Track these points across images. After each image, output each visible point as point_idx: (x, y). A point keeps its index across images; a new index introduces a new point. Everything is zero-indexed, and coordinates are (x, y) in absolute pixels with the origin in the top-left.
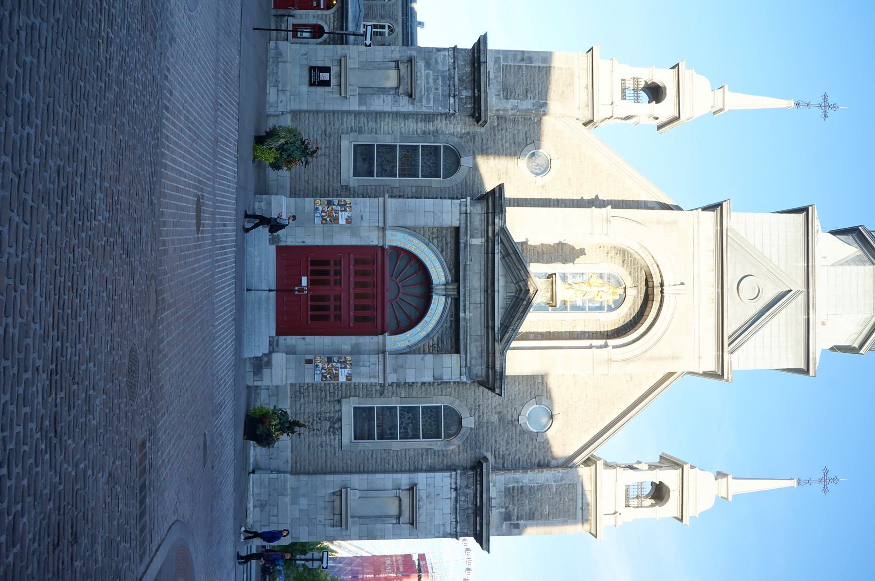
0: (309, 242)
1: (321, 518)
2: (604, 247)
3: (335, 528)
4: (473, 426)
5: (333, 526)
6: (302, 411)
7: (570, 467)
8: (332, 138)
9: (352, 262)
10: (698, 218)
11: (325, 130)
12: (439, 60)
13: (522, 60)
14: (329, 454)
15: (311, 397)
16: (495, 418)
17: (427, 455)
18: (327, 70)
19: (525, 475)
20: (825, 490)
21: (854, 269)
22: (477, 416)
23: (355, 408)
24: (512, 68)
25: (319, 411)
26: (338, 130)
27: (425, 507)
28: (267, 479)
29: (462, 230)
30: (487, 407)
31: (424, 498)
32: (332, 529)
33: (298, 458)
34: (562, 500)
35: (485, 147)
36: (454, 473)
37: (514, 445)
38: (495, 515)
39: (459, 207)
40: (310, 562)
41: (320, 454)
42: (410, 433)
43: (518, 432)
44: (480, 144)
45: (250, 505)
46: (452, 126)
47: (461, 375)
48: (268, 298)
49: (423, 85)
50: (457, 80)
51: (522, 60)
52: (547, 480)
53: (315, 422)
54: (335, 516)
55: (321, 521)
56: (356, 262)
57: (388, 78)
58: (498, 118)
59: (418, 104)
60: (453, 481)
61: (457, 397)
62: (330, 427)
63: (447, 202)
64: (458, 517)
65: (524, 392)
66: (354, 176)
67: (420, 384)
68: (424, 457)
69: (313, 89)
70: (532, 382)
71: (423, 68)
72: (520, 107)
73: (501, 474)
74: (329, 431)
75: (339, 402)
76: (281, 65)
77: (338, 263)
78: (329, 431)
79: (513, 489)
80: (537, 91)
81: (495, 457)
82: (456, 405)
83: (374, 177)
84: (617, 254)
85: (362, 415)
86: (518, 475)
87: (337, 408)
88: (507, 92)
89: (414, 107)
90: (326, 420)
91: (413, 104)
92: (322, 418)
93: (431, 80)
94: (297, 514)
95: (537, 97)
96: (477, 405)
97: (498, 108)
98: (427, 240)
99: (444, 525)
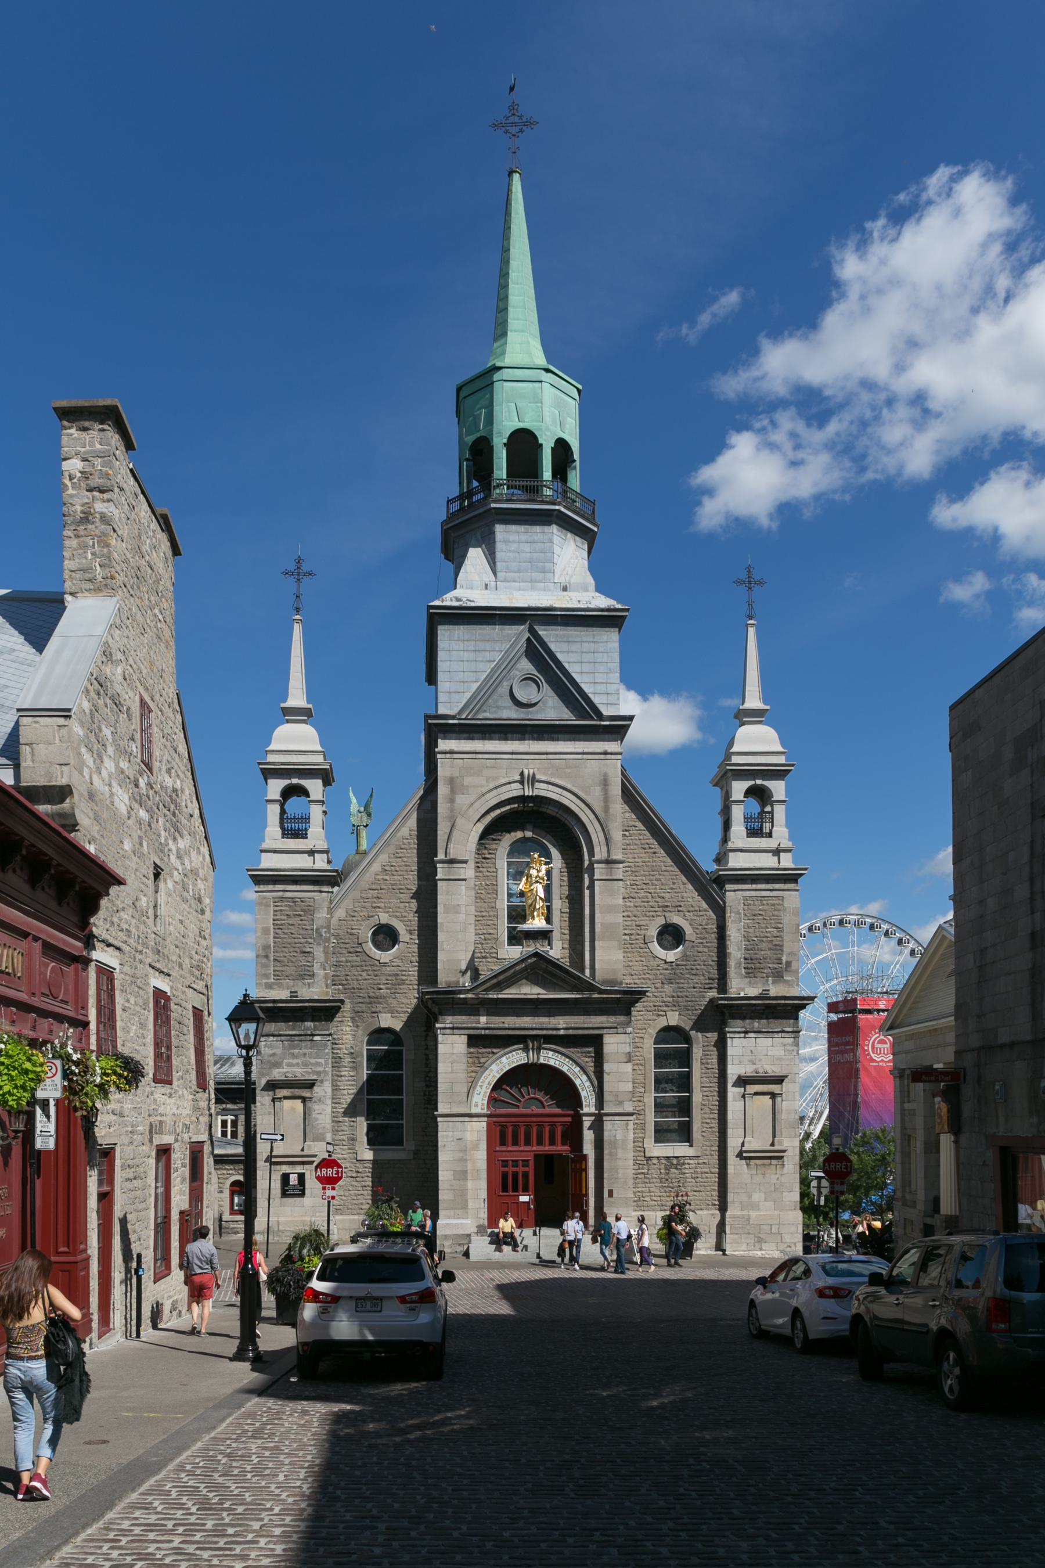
0: (484, 1194)
1: (774, 1178)
2: (478, 863)
4: (677, 1013)
6: (659, 1198)
7: (724, 902)
8: (360, 1170)
9: (504, 1148)
10: (446, 753)
11: (352, 1177)
12: (271, 1052)
13: (267, 957)
14: (704, 1170)
15: (644, 1189)
16: (668, 989)
17: (708, 1064)
18: (285, 1178)
20: (760, 583)
21: (499, 546)
22: (665, 1009)
23: (656, 1141)
24: (276, 968)
25: (659, 1181)
26: (352, 1163)
27: (765, 1066)
28: (732, 1236)
30: (656, 997)
31: (755, 1067)
32: (786, 1166)
33: (710, 1203)
34: (761, 913)
35: (367, 1000)
36: (728, 1035)
37: (698, 967)
38: (775, 990)
40: (822, 1190)
41: (706, 1180)
42: (685, 1083)
43: (684, 963)
44: (364, 1005)
45: (759, 1253)
46: (345, 1037)
48: (546, 1237)
49: (300, 1070)
50: (294, 1033)
51: (267, 957)
53: (671, 1185)
56: (503, 1143)
57: (293, 1109)
58: (334, 985)
59: (323, 1075)
60: (737, 1035)
61: (644, 1031)
62: (676, 1168)
63: (442, 1049)
64: (776, 1030)
65: (640, 956)
66: (403, 1145)
68: (710, 1066)
69: (307, 1191)
70: (628, 946)
71: (281, 1070)
72: (322, 959)
75: (649, 1159)
76: (281, 1228)
77: (505, 1163)
79: (748, 968)
80: (303, 940)
81: (711, 988)
82: (653, 1032)
83: (402, 1124)
84: (485, 848)
85: (662, 1134)
87: (655, 1161)
88: (306, 975)
89: (326, 1080)
91: (322, 1081)
93: (295, 1061)
94: (770, 1204)
95: (310, 940)
96: (653, 1008)
97: (323, 985)
98: (482, 1070)
99: (784, 1045)
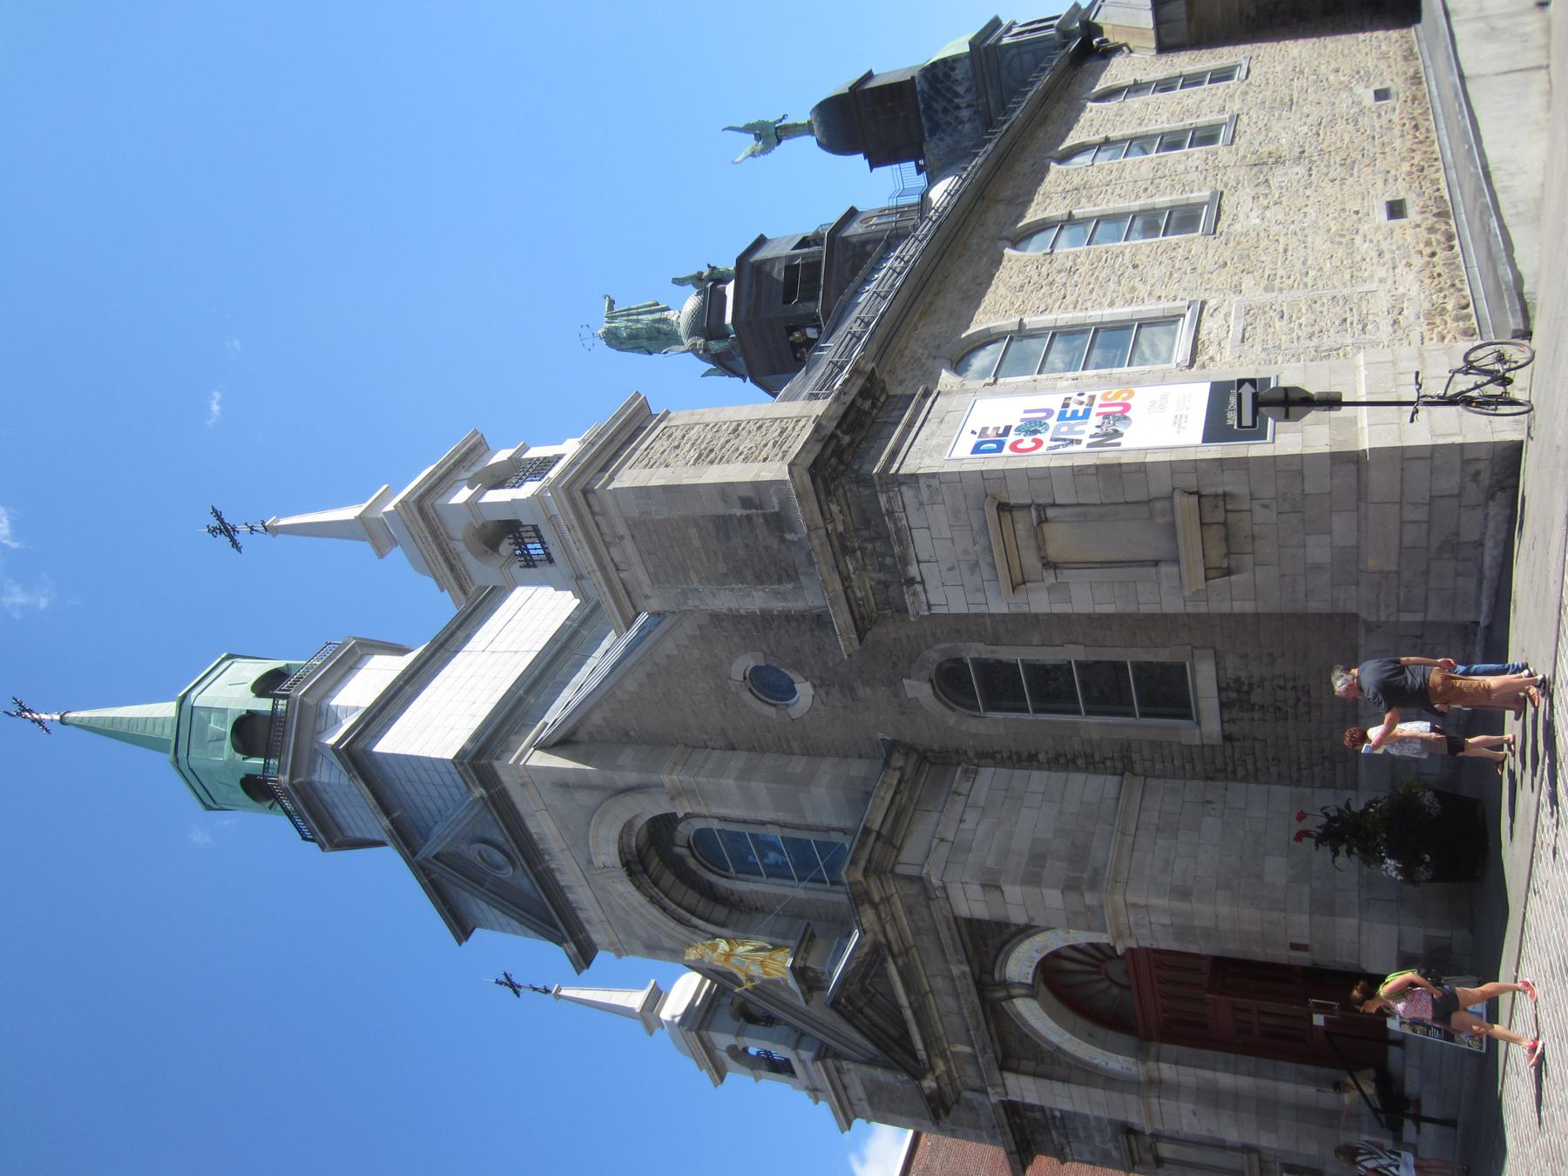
3: (1220, 491)
5: (1225, 495)
16: (863, 692)
19: (763, 606)
29: (995, 1067)
32: (1228, 489)
39: (1009, 1091)
47: (944, 888)
52: (714, 595)
54: (1222, 520)
55: (1265, 506)
62: (1248, 692)
67: (1041, 757)
73: (818, 608)
74: (1250, 685)
75: (1228, 738)
78: (1250, 685)
86: (778, 605)
90: (1262, 707)
92: (1271, 709)
99: (921, 504)
